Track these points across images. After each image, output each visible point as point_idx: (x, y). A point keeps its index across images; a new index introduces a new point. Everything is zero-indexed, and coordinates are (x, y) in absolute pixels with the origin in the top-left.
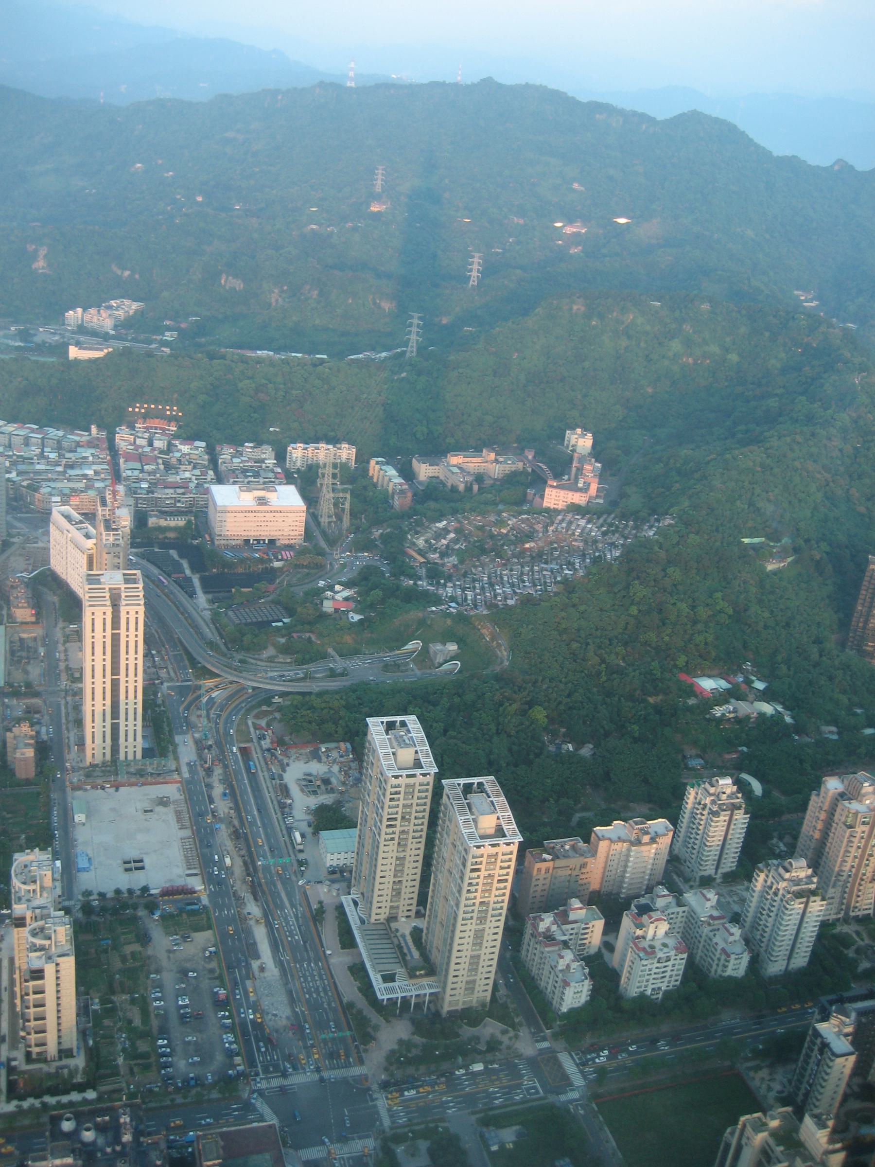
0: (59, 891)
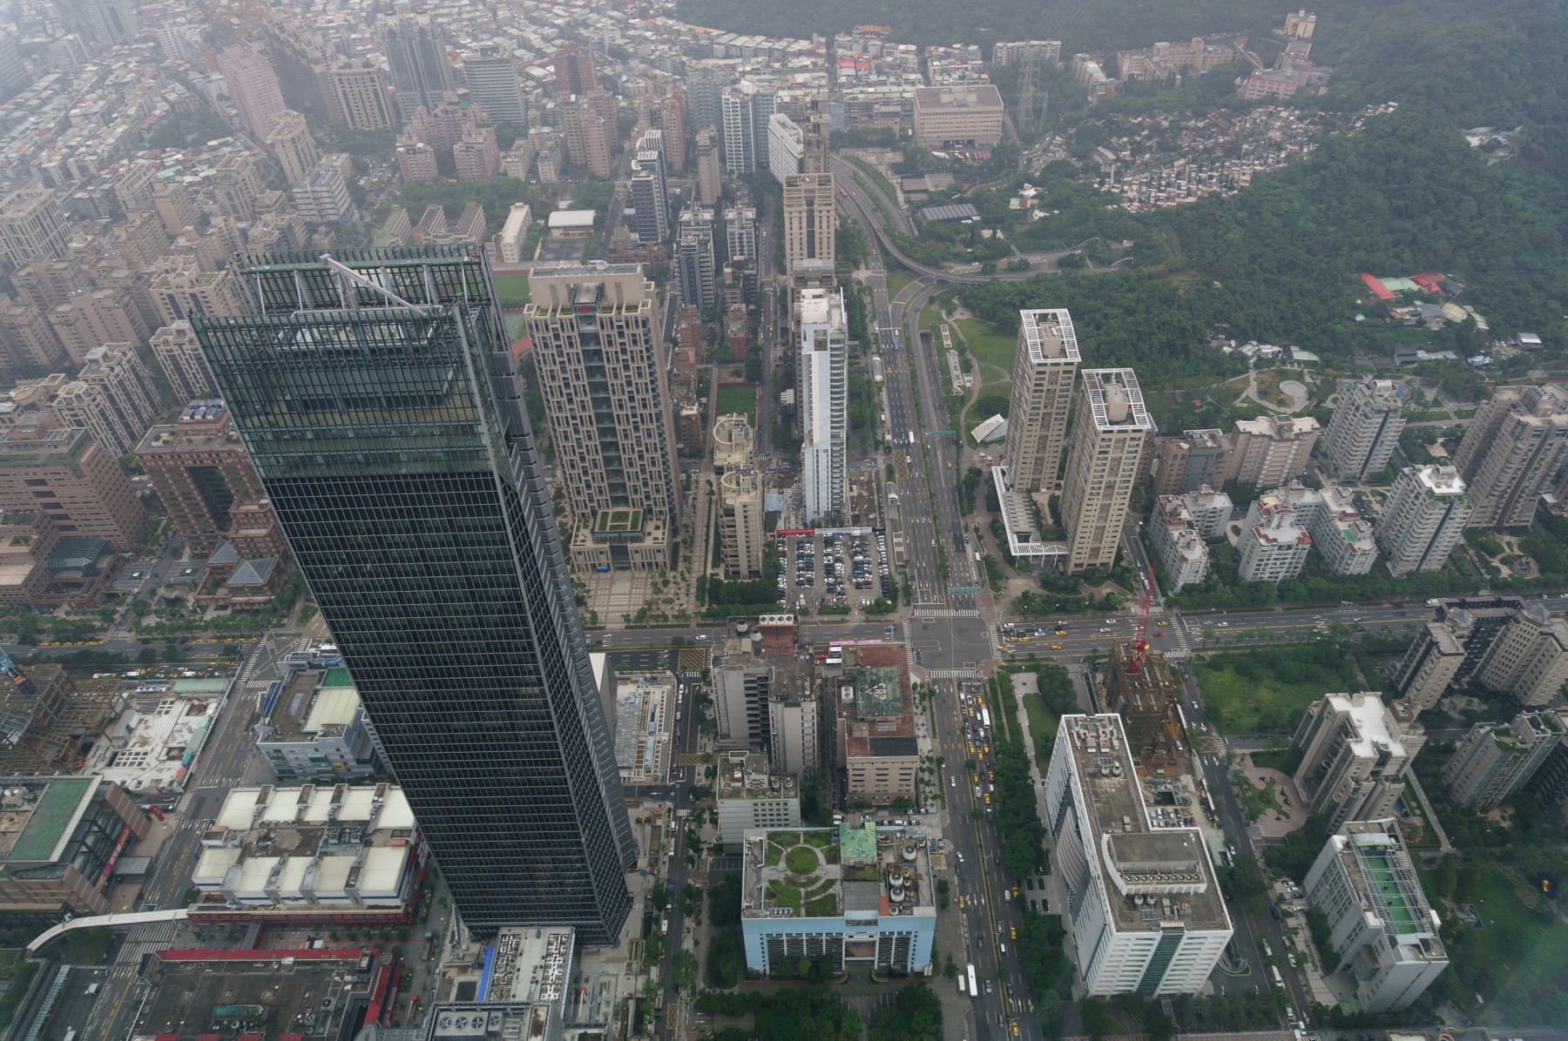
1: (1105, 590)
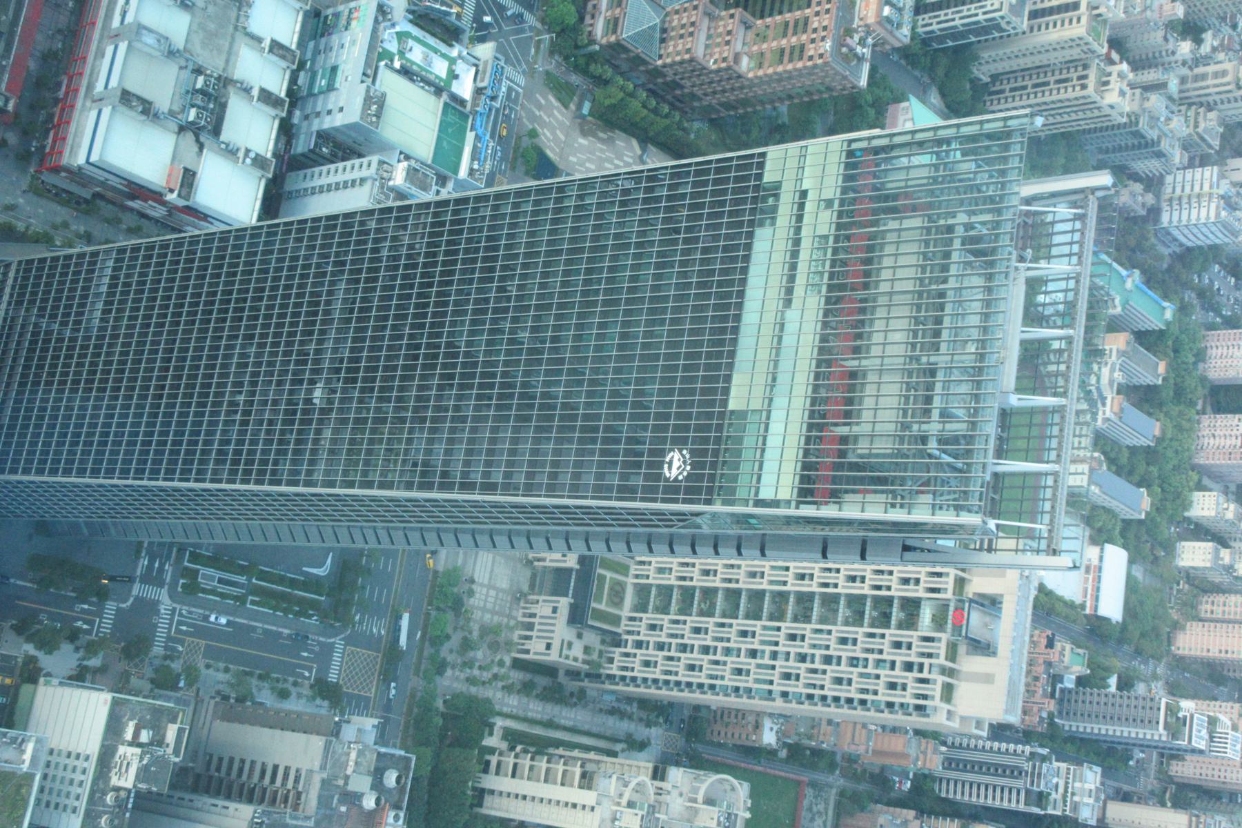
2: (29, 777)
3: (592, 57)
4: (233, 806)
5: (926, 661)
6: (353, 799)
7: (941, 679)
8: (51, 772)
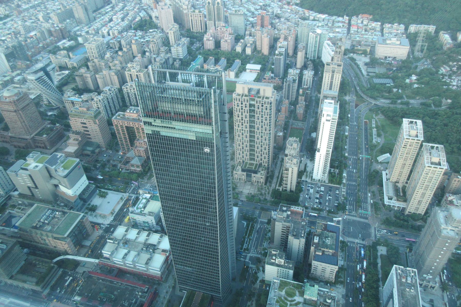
0: (298, 150)
1: (419, 223)
2: (281, 280)
3: (144, 171)
4: (289, 240)
5: (261, 102)
6: (288, 216)
7: (264, 99)
8: (281, 277)
